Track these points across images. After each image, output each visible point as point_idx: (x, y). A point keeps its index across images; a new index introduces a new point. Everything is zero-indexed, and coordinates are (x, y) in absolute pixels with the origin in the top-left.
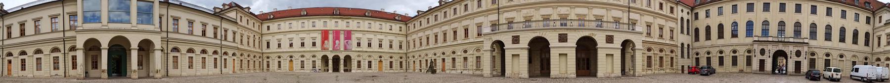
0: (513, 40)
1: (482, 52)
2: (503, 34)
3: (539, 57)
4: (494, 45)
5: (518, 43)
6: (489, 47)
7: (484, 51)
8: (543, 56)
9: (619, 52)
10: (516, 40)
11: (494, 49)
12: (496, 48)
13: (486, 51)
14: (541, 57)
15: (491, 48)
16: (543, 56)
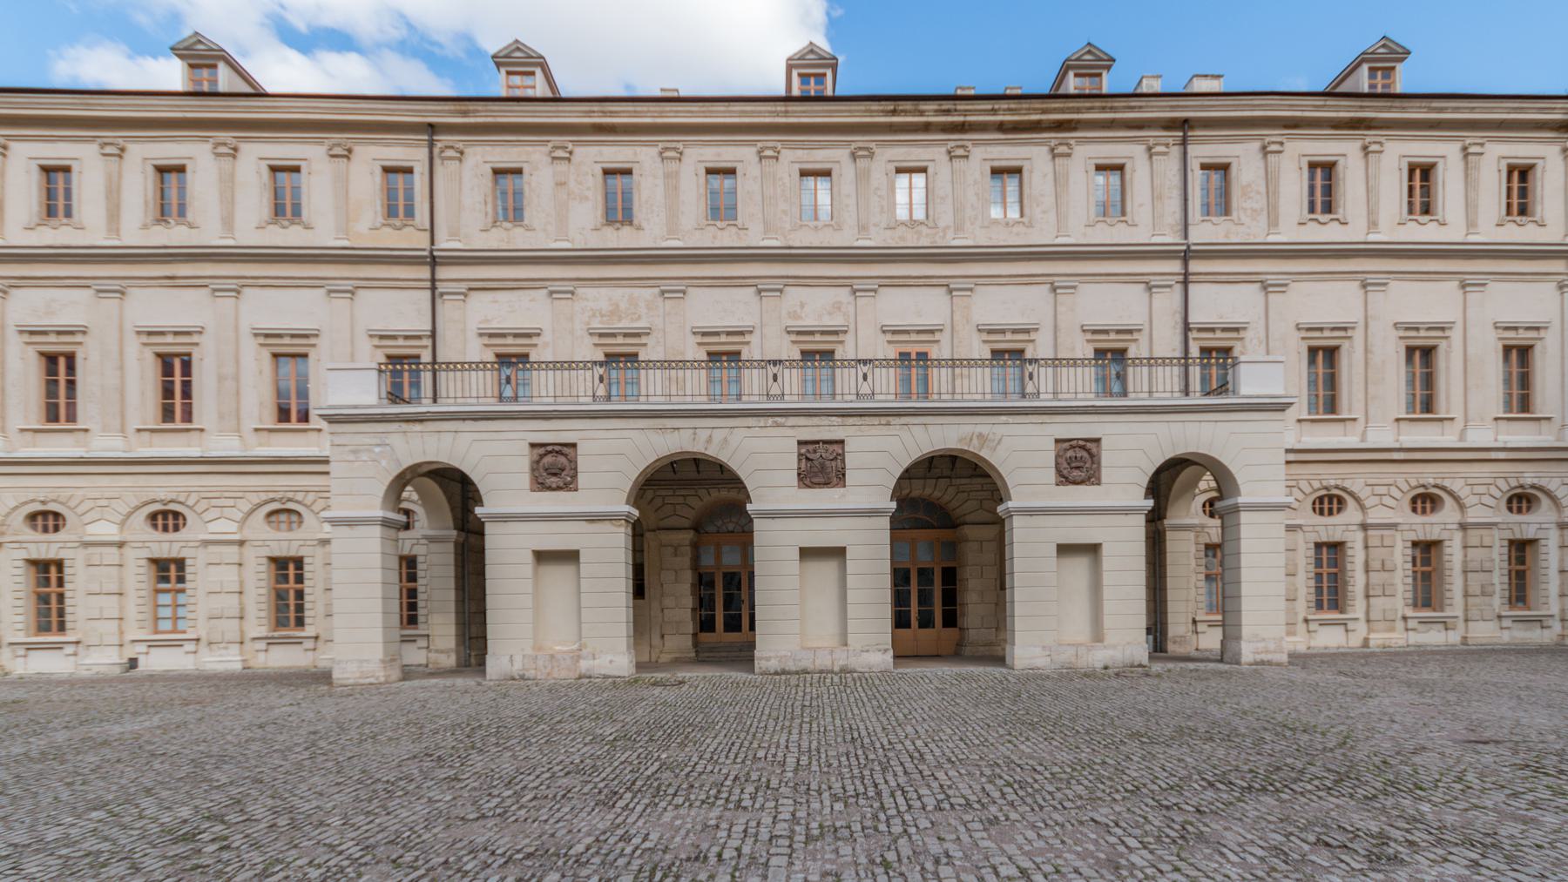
0: (535, 466)
1: (313, 528)
2: (469, 425)
3: (685, 560)
4: (409, 492)
5: (570, 485)
6: (378, 501)
7: (335, 522)
8: (708, 561)
9: (1136, 528)
10: (555, 472)
11: (407, 512)
12: (419, 510)
13: (350, 523)
14: (696, 559)
15: (385, 505)
16: (708, 561)
